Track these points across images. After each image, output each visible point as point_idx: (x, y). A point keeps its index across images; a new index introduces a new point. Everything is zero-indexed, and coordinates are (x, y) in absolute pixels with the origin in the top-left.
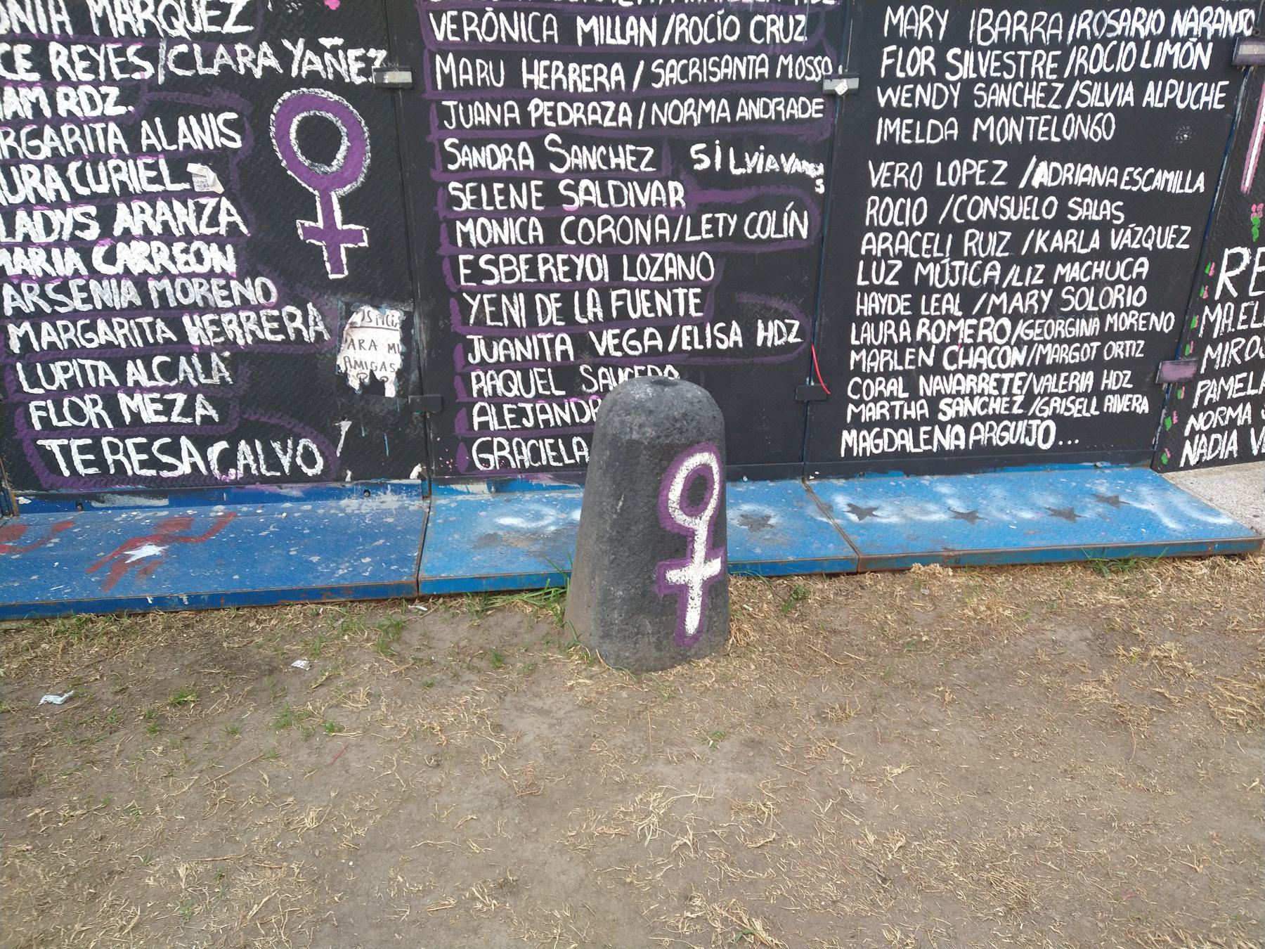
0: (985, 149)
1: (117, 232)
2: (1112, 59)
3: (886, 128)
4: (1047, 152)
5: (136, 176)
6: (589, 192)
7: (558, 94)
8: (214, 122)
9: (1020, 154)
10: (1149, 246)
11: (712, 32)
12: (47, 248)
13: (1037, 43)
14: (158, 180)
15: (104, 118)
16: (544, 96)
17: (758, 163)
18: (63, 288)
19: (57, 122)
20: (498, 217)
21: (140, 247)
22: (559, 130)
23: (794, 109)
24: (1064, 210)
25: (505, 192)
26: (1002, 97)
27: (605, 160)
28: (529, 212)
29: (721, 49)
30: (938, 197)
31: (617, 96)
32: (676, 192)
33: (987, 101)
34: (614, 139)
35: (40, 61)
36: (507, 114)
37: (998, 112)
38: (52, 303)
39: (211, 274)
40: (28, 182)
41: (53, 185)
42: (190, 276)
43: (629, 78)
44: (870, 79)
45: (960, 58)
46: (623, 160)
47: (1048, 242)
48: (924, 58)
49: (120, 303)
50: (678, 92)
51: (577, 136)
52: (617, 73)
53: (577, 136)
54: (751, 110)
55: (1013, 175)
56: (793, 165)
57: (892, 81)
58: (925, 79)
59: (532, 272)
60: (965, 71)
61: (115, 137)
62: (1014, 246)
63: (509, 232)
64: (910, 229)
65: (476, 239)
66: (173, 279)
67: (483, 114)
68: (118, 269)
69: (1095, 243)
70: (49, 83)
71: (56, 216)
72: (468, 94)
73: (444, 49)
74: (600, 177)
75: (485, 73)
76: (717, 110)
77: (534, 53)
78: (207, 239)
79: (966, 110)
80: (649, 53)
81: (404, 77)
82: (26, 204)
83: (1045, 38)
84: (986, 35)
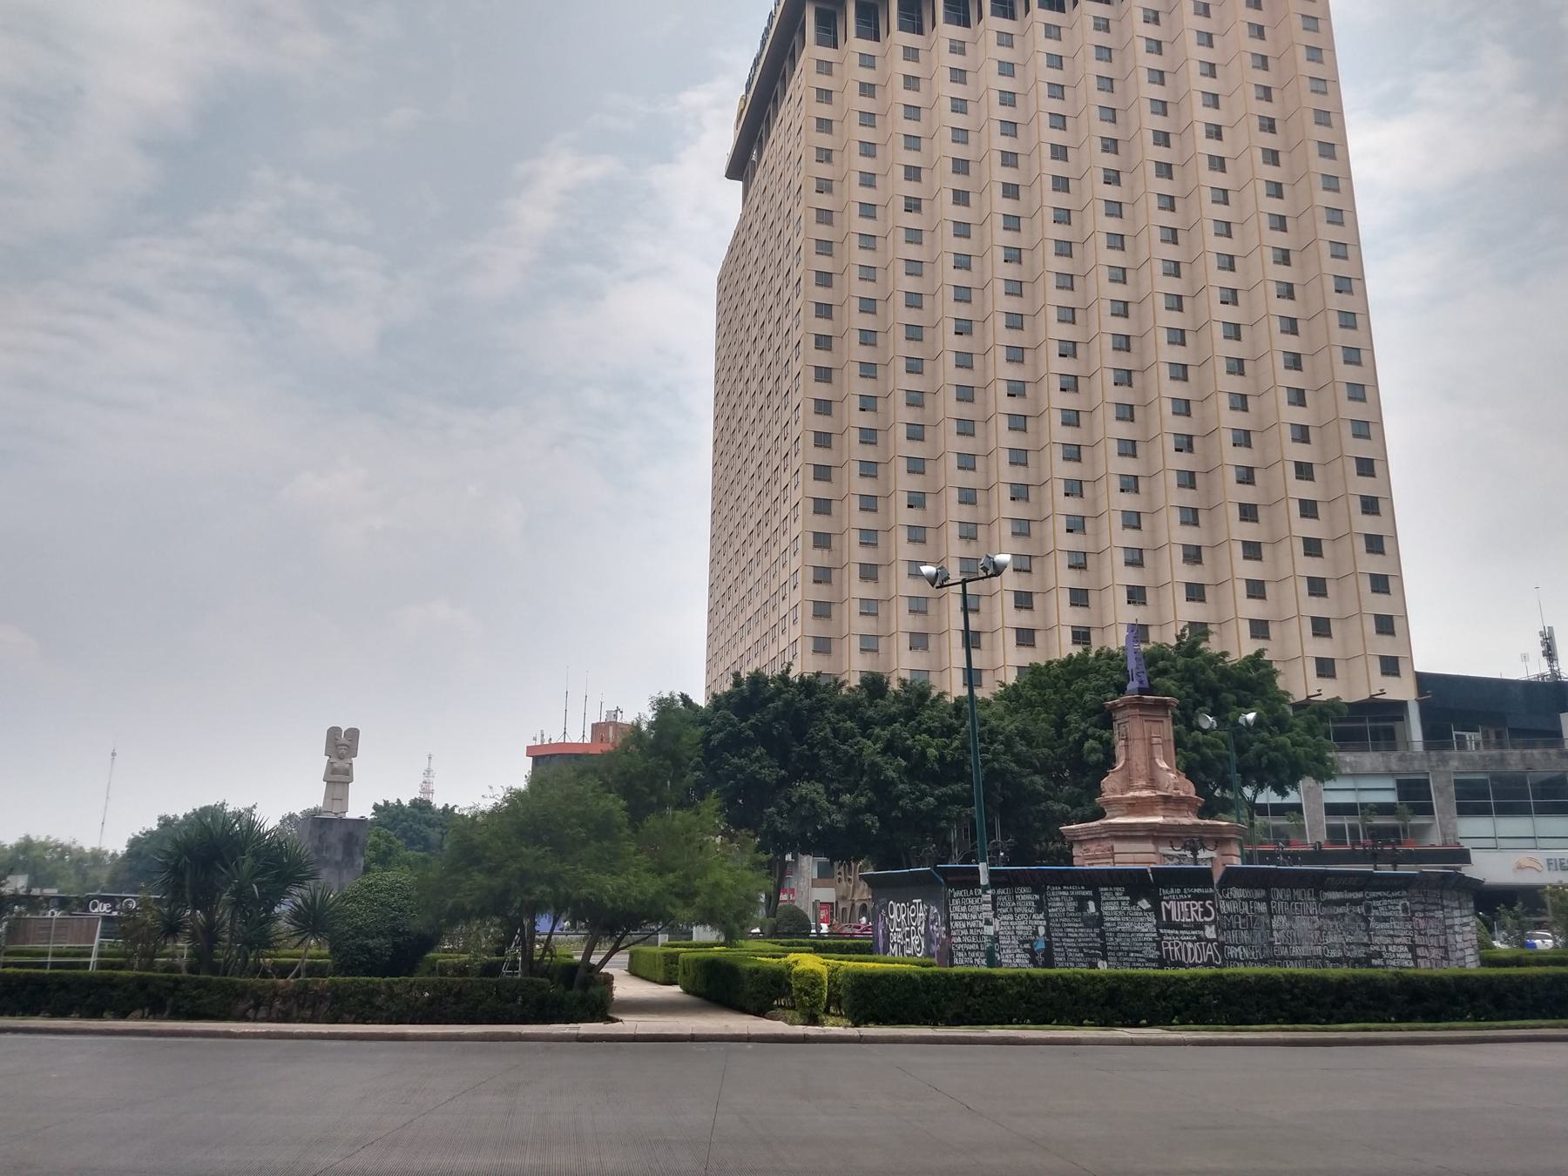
3: (1108, 948)
5: (1019, 951)
6: (1071, 955)
9: (1129, 952)
23: (1096, 945)
26: (1124, 944)
30: (1118, 957)
32: (1082, 955)
34: (1074, 948)
36: (1060, 944)
41: (1009, 951)
46: (1075, 950)
48: (1112, 939)
53: (1068, 947)
67: (1057, 944)
72: (1056, 942)
75: (1057, 939)
79: (1119, 946)
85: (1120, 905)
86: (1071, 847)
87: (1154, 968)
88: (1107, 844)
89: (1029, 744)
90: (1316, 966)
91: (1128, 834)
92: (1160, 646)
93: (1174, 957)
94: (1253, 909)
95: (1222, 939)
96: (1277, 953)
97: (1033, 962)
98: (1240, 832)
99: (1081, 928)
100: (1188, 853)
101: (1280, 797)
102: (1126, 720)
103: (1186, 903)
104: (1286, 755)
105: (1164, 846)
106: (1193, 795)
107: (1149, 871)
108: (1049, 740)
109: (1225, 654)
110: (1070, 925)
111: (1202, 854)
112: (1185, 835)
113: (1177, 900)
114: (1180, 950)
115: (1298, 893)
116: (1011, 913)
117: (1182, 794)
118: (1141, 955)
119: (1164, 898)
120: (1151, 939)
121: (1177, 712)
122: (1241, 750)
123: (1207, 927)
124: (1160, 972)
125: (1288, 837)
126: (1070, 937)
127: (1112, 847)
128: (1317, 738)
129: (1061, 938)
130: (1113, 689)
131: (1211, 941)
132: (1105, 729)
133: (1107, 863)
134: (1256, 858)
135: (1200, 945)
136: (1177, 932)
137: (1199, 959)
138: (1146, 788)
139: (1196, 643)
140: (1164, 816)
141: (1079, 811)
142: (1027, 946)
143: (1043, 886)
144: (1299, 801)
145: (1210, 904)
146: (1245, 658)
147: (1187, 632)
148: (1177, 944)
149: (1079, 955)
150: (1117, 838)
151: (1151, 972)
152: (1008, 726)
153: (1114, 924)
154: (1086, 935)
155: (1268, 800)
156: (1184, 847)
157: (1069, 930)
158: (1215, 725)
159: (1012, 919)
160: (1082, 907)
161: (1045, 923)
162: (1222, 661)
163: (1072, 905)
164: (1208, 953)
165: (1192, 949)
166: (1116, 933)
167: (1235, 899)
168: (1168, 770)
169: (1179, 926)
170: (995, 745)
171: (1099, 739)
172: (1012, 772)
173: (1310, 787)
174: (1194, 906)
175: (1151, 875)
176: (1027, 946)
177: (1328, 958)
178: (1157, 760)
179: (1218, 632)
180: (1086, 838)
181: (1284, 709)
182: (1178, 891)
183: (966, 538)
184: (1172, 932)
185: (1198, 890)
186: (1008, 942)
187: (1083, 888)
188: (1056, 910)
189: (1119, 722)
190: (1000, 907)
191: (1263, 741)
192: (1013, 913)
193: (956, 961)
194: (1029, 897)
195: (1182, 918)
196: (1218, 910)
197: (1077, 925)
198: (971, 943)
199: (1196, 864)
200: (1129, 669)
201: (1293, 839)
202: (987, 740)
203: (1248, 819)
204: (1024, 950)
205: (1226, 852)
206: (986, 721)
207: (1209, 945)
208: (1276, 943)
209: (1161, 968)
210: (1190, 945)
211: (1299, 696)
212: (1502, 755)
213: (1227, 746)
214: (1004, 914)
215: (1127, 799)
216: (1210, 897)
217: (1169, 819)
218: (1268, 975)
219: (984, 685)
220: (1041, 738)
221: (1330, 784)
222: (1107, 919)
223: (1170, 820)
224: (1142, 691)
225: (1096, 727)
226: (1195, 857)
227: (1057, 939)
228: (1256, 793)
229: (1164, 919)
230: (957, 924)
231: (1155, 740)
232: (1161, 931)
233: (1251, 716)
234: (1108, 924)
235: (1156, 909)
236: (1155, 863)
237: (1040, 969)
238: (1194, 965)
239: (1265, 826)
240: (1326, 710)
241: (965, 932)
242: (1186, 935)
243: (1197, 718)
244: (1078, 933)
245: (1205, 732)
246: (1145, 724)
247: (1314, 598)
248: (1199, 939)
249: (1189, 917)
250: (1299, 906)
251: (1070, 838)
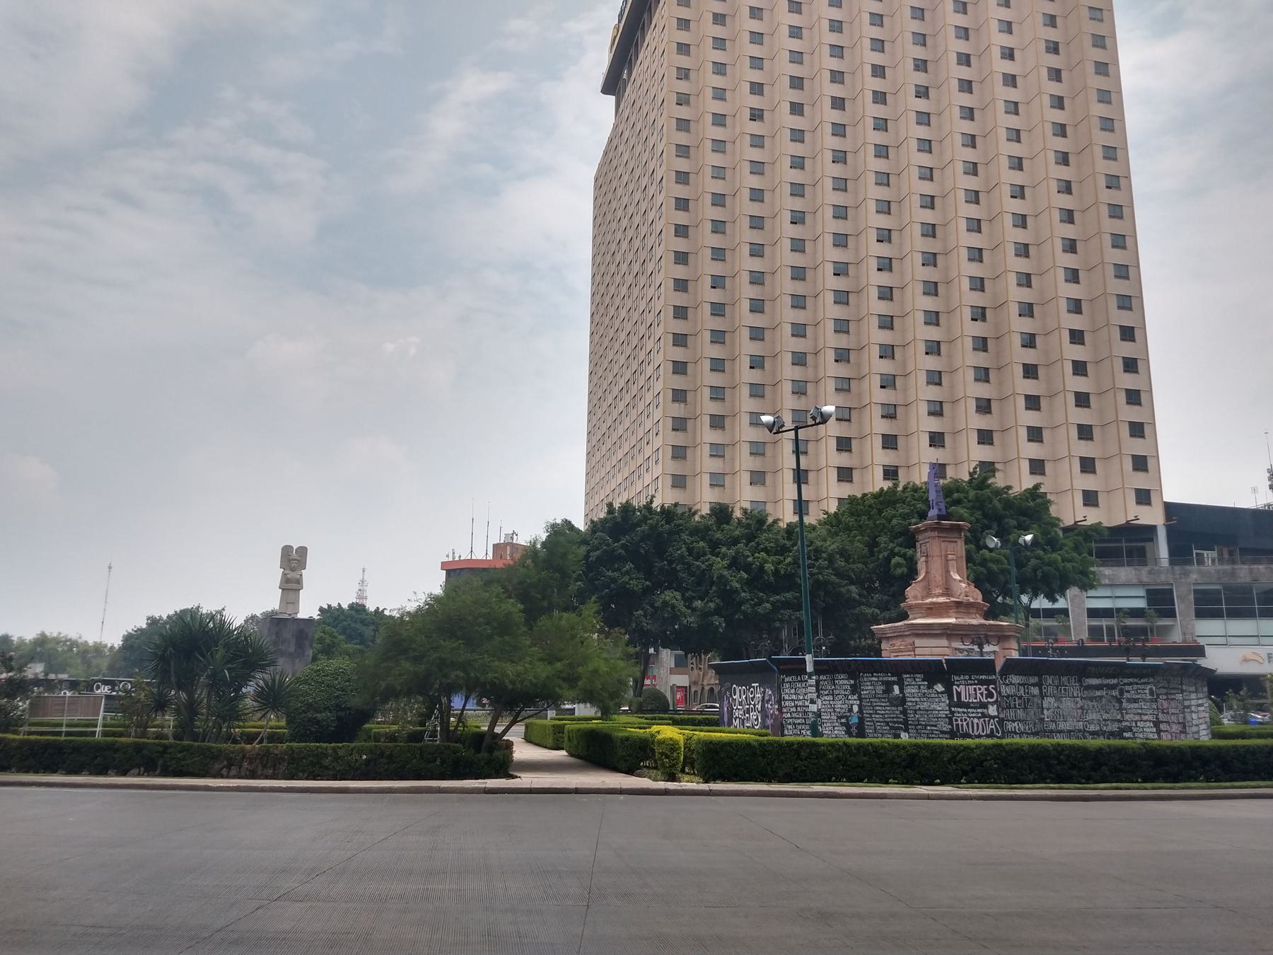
0: (921, 725)
5: (837, 724)
9: (926, 726)
17: (896, 725)
23: (900, 720)
32: (888, 728)
34: (881, 722)
41: (830, 725)
46: (882, 724)
48: (912, 715)
54: (895, 720)
63: (871, 731)
67: (868, 719)
75: (868, 716)
79: (918, 721)
86: (880, 643)
87: (947, 739)
88: (909, 640)
89: (847, 561)
90: (1078, 738)
91: (926, 632)
92: (956, 481)
93: (963, 731)
94: (1028, 692)
95: (1001, 716)
96: (1046, 727)
97: (849, 733)
98: (1018, 630)
99: (887, 706)
100: (976, 648)
101: (1051, 603)
102: (927, 540)
103: (973, 687)
104: (1057, 569)
105: (953, 641)
106: (980, 600)
107: (944, 661)
108: (863, 557)
109: (1009, 488)
110: (879, 704)
111: (987, 648)
112: (974, 633)
113: (966, 685)
114: (967, 724)
115: (1064, 679)
117: (971, 600)
118: (935, 728)
119: (956, 683)
120: (944, 716)
121: (969, 534)
122: (1020, 565)
123: (990, 706)
124: (951, 742)
125: (1056, 635)
126: (878, 714)
127: (914, 642)
128: (1083, 555)
130: (916, 516)
131: (993, 717)
132: (909, 549)
133: (909, 655)
134: (1030, 651)
135: (984, 721)
136: (965, 710)
137: (983, 732)
138: (942, 595)
139: (986, 479)
140: (956, 618)
142: (843, 720)
143: (858, 673)
144: (1066, 607)
145: (992, 688)
146: (1025, 491)
147: (978, 469)
148: (966, 720)
149: (885, 728)
150: (918, 635)
151: (945, 742)
152: (829, 546)
153: (914, 704)
155: (1041, 606)
156: (973, 643)
157: (878, 708)
158: (999, 545)
159: (831, 699)
160: (888, 690)
161: (858, 702)
162: (1006, 493)
163: (880, 689)
164: (990, 727)
165: (977, 724)
166: (915, 710)
167: (1014, 684)
168: (960, 581)
169: (967, 705)
170: (820, 561)
172: (833, 584)
173: (1075, 595)
174: (980, 689)
175: (945, 665)
176: (843, 720)
177: (1088, 732)
178: (952, 573)
179: (1004, 469)
180: (892, 635)
181: (1056, 532)
182: (967, 677)
183: (797, 393)
184: (962, 710)
185: (983, 677)
186: (828, 718)
187: (889, 675)
189: (921, 542)
190: (822, 690)
191: (1038, 558)
192: (833, 695)
193: (786, 732)
194: (845, 682)
195: (969, 699)
196: (999, 693)
197: (884, 704)
198: (799, 718)
199: (982, 656)
200: (930, 499)
201: (1060, 636)
202: (813, 558)
203: (1024, 621)
204: (841, 723)
205: (1007, 647)
206: (812, 542)
207: (992, 720)
208: (1046, 719)
209: (952, 738)
210: (976, 721)
211: (1068, 521)
212: (1233, 569)
213: (1008, 561)
214: (826, 695)
215: (927, 604)
216: (994, 682)
217: (960, 620)
218: (1039, 745)
220: (856, 557)
221: (1091, 593)
222: (909, 699)
223: (961, 621)
224: (940, 517)
225: (901, 546)
226: (981, 650)
227: (868, 716)
228: (1031, 600)
229: (955, 700)
230: (787, 704)
231: (950, 557)
232: (953, 709)
233: (1029, 538)
234: (910, 704)
235: (949, 691)
236: (948, 655)
237: (854, 739)
238: (979, 736)
239: (1039, 627)
240: (1089, 532)
241: (794, 709)
242: (973, 713)
243: (985, 538)
244: (885, 711)
245: (991, 550)
246: (943, 544)
247: (1082, 442)
248: (984, 715)
249: (976, 698)
250: (1065, 690)
251: (879, 636)
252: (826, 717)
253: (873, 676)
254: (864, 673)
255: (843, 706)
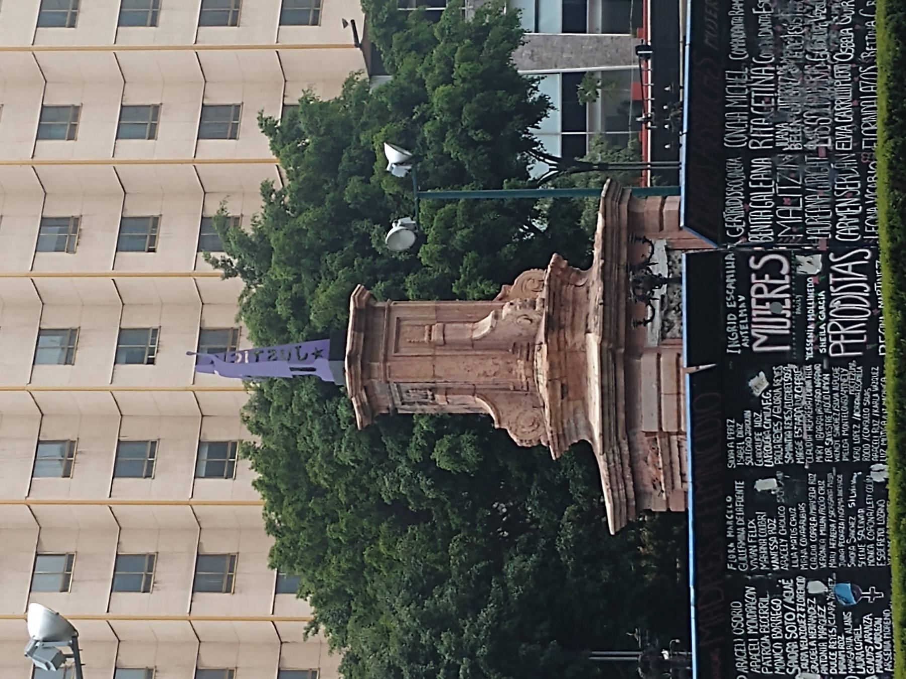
0: (850, 432)
1: (871, 642)
2: (827, 401)
4: (851, 414)
6: (861, 533)
7: (837, 539)
8: (845, 617)
9: (852, 421)
10: (877, 379)
11: (822, 503)
12: (875, 658)
13: (823, 422)
14: (859, 631)
15: (845, 640)
16: (838, 543)
18: (886, 657)
19: (846, 650)
20: (867, 555)
21: (875, 638)
22: (845, 540)
23: (840, 482)
24: (867, 407)
25: (861, 553)
26: (837, 429)
27: (852, 529)
28: (866, 548)
29: (826, 501)
30: (864, 442)
31: (837, 526)
33: (838, 433)
34: (847, 526)
35: (833, 651)
37: (841, 429)
38: (889, 660)
39: (882, 624)
40: (859, 659)
42: (883, 628)
43: (833, 523)
44: (834, 464)
45: (827, 442)
46: (853, 525)
47: (876, 409)
49: (890, 645)
50: (836, 511)
51: (847, 536)
52: (832, 526)
53: (847, 536)
54: (840, 493)
55: (857, 422)
56: (854, 481)
57: (833, 459)
58: (833, 450)
59: (881, 547)
60: (831, 440)
61: (849, 638)
62: (876, 418)
63: (872, 553)
64: (871, 448)
65: (873, 561)
66: (883, 633)
67: (842, 557)
68: (881, 644)
69: (876, 395)
70: (838, 650)
71: (868, 655)
72: (838, 561)
73: (828, 565)
74: (857, 530)
76: (840, 501)
77: (828, 545)
78: (873, 623)
80: (828, 518)
81: (834, 574)
82: (866, 660)
83: (822, 420)
84: (822, 435)
85: (761, 430)
86: (649, 512)
87: (882, 375)
88: (643, 444)
89: (441, 580)
90: (873, 78)
91: (622, 403)
92: (245, 309)
93: (860, 336)
94: (765, 182)
95: (823, 247)
96: (847, 145)
97: (879, 608)
98: (615, 194)
99: (808, 509)
100: (658, 293)
101: (550, 112)
102: (394, 388)
103: (754, 305)
104: (468, 95)
105: (645, 338)
106: (545, 275)
107: (693, 369)
108: (433, 538)
109: (267, 190)
111: (660, 268)
112: (623, 295)
113: (750, 323)
114: (846, 324)
115: (733, 99)
116: (784, 647)
117: (544, 294)
118: (858, 399)
119: (745, 345)
121: (380, 286)
122: (458, 177)
123: (800, 270)
124: (890, 366)
125: (627, 103)
126: (828, 531)
127: (648, 434)
128: (436, 34)
129: (829, 551)
130: (330, 406)
131: (827, 263)
132: (413, 426)
133: (679, 447)
134: (665, 165)
135: (836, 285)
136: (811, 327)
137: (862, 289)
138: (530, 359)
139: (243, 240)
140: (588, 332)
141: (577, 490)
142: (848, 619)
144: (559, 78)
145: (756, 262)
146: (277, 153)
147: (218, 256)
148: (834, 328)
150: (631, 424)
151: (889, 382)
152: (401, 622)
153: (800, 444)
154: (822, 499)
155: (557, 134)
156: (648, 300)
157: (813, 533)
158: (407, 220)
160: (767, 503)
161: (801, 580)
162: (280, 195)
163: (765, 524)
164: (850, 272)
165: (843, 301)
166: (816, 443)
167: (747, 215)
168: (496, 317)
169: (800, 322)
170: (441, 650)
171: (431, 439)
172: (498, 618)
173: (531, 57)
174: (759, 291)
175: (701, 367)
176: (848, 619)
177: (857, 55)
178: (476, 335)
179: (221, 198)
180: (630, 484)
181: (379, 92)
182: (732, 318)
184: (811, 336)
185: (730, 281)
186: (842, 657)
187: (729, 499)
188: (774, 555)
189: (398, 402)
190: (772, 669)
191: (441, 134)
192: (784, 641)
194: (751, 608)
195: (784, 316)
196: (768, 247)
197: (804, 517)
199: (680, 281)
200: (290, 375)
201: (630, 94)
202: (431, 666)
203: (591, 173)
204: (855, 626)
205: (656, 222)
206: (390, 667)
207: (834, 268)
208: (829, 145)
209: (881, 361)
210: (836, 304)
211: (356, 61)
213: (450, 201)
215: (552, 398)
216: (742, 260)
217: (592, 323)
218: (891, 167)
219: (314, 666)
220: (429, 556)
221: (527, 21)
222: (789, 457)
223: (595, 322)
224: (337, 354)
225: (406, 444)
226: (666, 281)
228: (541, 154)
229: (788, 348)
231: (436, 336)
232: (809, 356)
233: (392, 155)
235: (768, 363)
236: (679, 355)
237: (893, 598)
238: (873, 299)
239: (606, 143)
240: (384, 16)
242: (817, 310)
243: (391, 252)
244: (818, 517)
245: (421, 239)
246: (403, 351)
247: (162, 17)
248: (824, 285)
249: (782, 301)
250: (758, 99)
251: (633, 512)
252: (841, 664)
253: (735, 541)
254: (727, 561)
255: (812, 619)
